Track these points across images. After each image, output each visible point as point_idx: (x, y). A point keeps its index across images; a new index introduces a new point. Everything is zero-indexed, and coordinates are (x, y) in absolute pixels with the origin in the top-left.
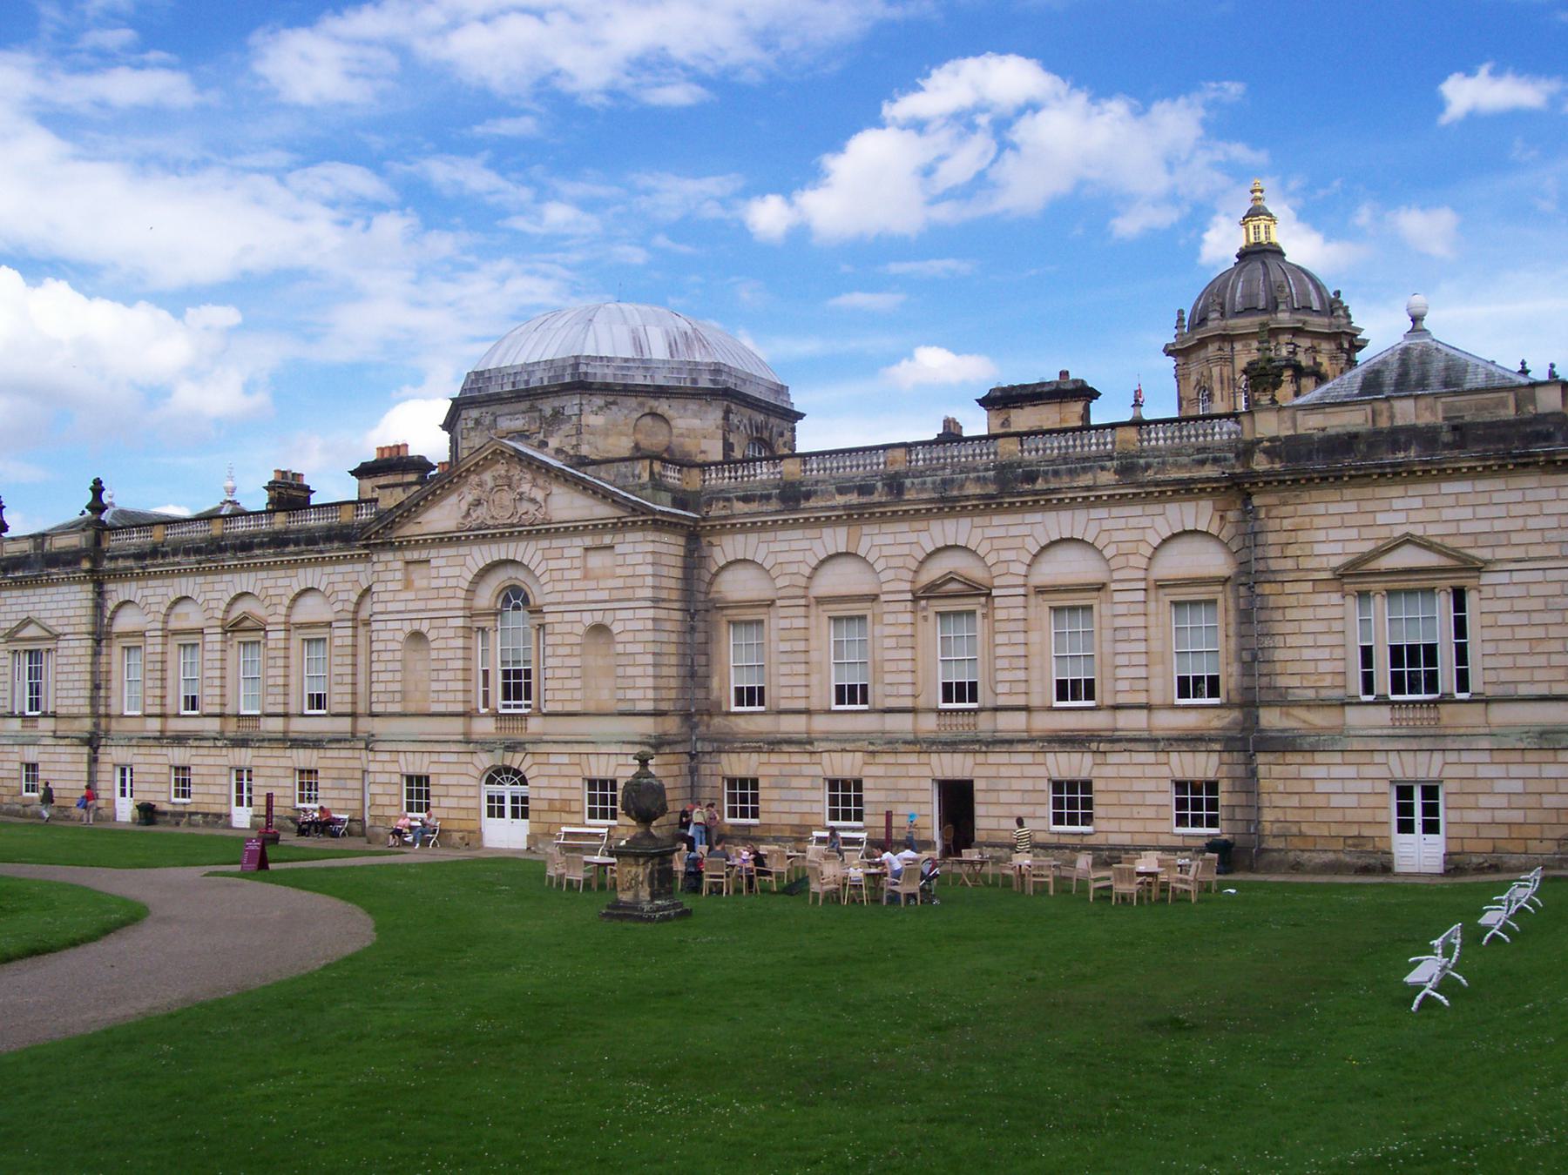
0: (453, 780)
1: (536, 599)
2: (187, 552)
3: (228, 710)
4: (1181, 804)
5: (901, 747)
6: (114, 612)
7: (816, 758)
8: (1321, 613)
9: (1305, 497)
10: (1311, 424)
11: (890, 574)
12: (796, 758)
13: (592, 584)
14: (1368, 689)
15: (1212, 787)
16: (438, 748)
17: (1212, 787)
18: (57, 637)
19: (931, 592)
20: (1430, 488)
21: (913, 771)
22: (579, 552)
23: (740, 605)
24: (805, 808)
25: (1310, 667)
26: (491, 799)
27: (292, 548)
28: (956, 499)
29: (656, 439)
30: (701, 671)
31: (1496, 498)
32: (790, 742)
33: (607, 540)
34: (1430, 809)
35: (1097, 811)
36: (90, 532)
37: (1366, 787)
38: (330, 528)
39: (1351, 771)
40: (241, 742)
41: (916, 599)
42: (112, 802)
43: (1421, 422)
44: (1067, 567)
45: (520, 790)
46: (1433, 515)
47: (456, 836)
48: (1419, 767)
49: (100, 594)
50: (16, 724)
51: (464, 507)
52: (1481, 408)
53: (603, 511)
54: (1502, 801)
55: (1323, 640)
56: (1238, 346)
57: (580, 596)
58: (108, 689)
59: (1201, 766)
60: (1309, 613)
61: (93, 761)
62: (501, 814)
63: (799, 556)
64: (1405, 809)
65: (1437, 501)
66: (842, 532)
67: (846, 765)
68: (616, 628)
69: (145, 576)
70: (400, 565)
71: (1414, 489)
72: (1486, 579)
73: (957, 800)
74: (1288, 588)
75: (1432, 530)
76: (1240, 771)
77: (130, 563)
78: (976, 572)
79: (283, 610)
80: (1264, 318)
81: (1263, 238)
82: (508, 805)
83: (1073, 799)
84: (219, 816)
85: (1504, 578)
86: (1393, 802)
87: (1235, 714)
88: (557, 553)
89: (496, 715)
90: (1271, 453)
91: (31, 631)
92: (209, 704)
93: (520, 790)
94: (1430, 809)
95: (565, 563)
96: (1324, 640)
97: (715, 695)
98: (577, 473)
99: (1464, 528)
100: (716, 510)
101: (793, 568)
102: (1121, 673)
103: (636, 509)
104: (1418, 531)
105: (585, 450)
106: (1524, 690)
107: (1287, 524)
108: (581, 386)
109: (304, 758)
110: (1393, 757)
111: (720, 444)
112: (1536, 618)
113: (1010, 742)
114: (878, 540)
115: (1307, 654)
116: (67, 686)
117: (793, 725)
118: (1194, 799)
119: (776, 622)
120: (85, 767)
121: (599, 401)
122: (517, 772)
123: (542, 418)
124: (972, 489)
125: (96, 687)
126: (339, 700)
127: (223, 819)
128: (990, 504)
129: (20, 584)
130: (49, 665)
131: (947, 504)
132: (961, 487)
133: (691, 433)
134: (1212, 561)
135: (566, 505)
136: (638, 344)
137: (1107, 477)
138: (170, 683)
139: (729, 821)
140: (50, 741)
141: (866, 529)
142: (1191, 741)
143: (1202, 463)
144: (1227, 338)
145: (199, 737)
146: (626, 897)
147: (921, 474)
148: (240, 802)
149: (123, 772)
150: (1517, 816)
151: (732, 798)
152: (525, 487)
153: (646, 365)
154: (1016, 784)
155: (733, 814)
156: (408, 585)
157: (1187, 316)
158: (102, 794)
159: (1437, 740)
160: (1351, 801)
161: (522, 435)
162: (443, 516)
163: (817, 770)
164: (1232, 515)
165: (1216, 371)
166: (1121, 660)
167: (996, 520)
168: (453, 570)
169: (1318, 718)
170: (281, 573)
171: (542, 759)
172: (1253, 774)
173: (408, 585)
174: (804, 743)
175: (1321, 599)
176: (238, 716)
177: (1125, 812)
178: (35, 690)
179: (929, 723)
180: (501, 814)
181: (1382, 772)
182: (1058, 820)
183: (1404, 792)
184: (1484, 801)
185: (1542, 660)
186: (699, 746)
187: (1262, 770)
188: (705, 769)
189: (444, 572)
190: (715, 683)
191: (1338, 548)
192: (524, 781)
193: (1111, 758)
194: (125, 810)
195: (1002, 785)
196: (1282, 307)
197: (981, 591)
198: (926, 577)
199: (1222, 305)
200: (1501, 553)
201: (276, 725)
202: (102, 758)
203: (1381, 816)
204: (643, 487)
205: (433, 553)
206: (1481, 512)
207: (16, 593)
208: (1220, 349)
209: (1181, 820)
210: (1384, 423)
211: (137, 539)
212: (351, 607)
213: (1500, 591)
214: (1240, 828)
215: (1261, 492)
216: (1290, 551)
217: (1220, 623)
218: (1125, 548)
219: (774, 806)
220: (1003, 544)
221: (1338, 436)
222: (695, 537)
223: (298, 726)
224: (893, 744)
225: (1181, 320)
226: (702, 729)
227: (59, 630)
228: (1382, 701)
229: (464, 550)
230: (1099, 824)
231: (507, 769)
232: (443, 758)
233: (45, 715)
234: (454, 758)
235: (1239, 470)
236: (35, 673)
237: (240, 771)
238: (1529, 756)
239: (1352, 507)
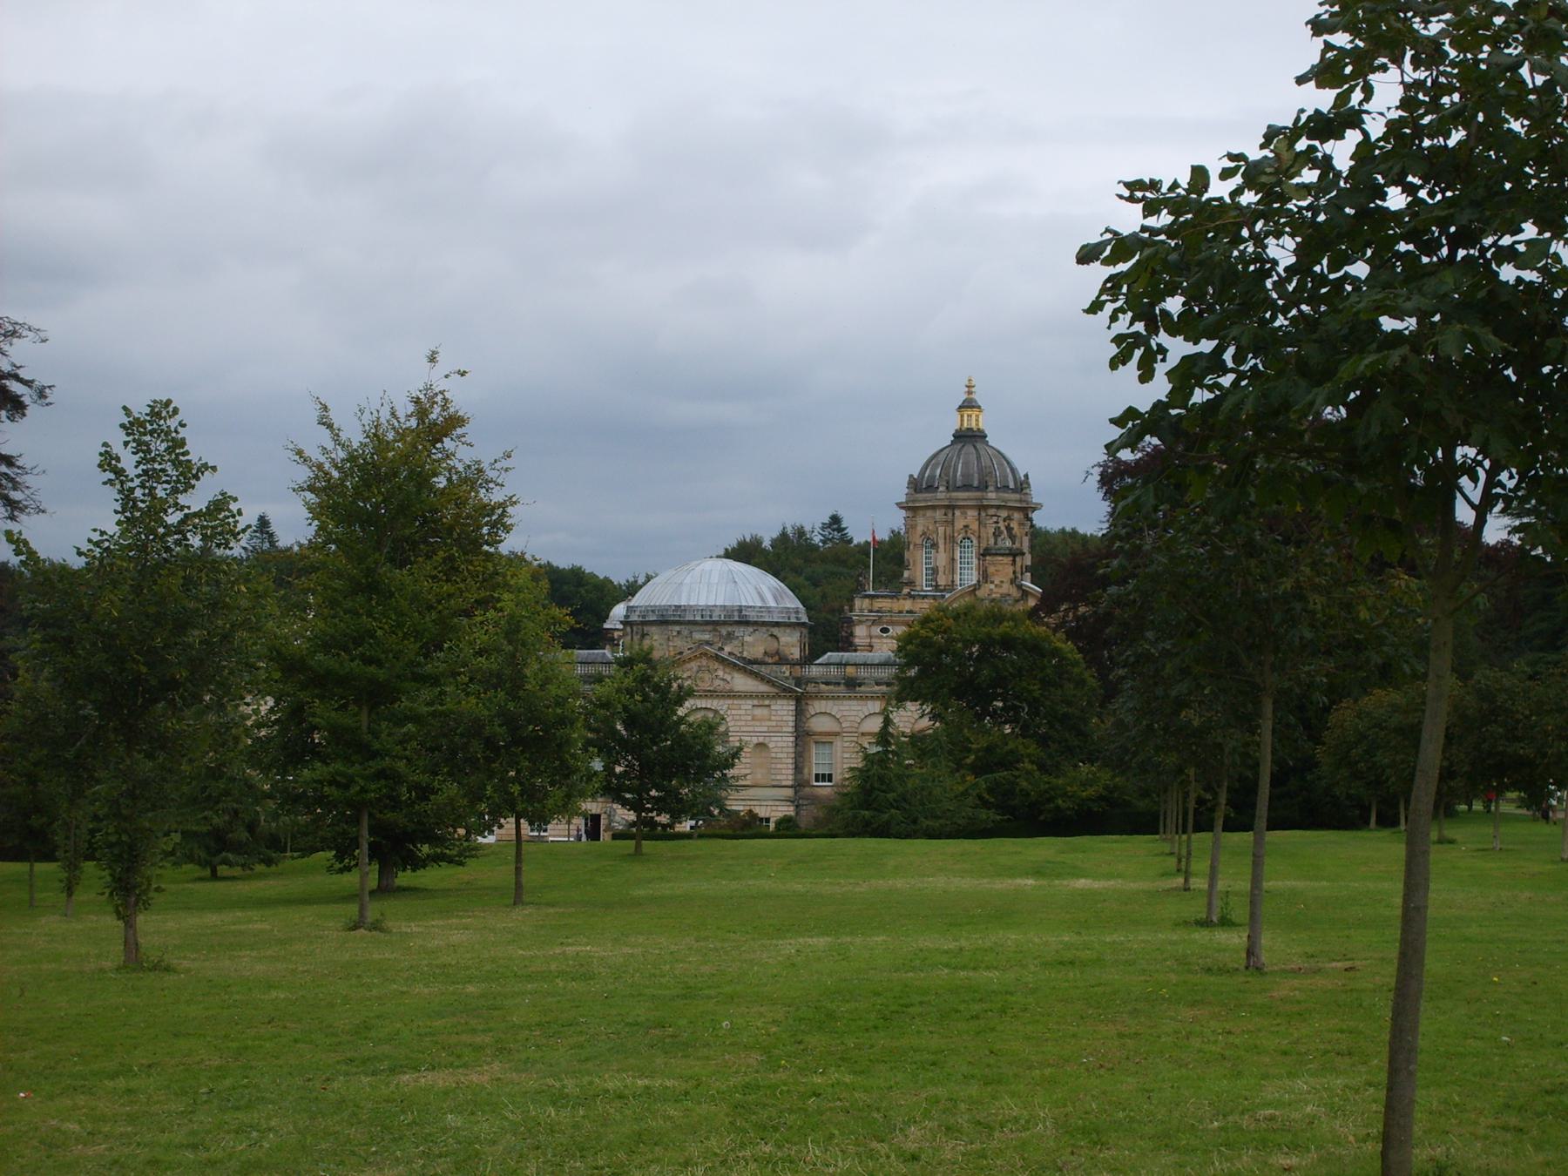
23: (820, 734)
53: (763, 688)
80: (978, 494)
81: (974, 425)
98: (747, 666)
100: (810, 688)
108: (745, 623)
119: (838, 743)
123: (721, 636)
133: (787, 645)
135: (741, 682)
152: (720, 673)
153: (769, 610)
165: (941, 530)
222: (800, 701)
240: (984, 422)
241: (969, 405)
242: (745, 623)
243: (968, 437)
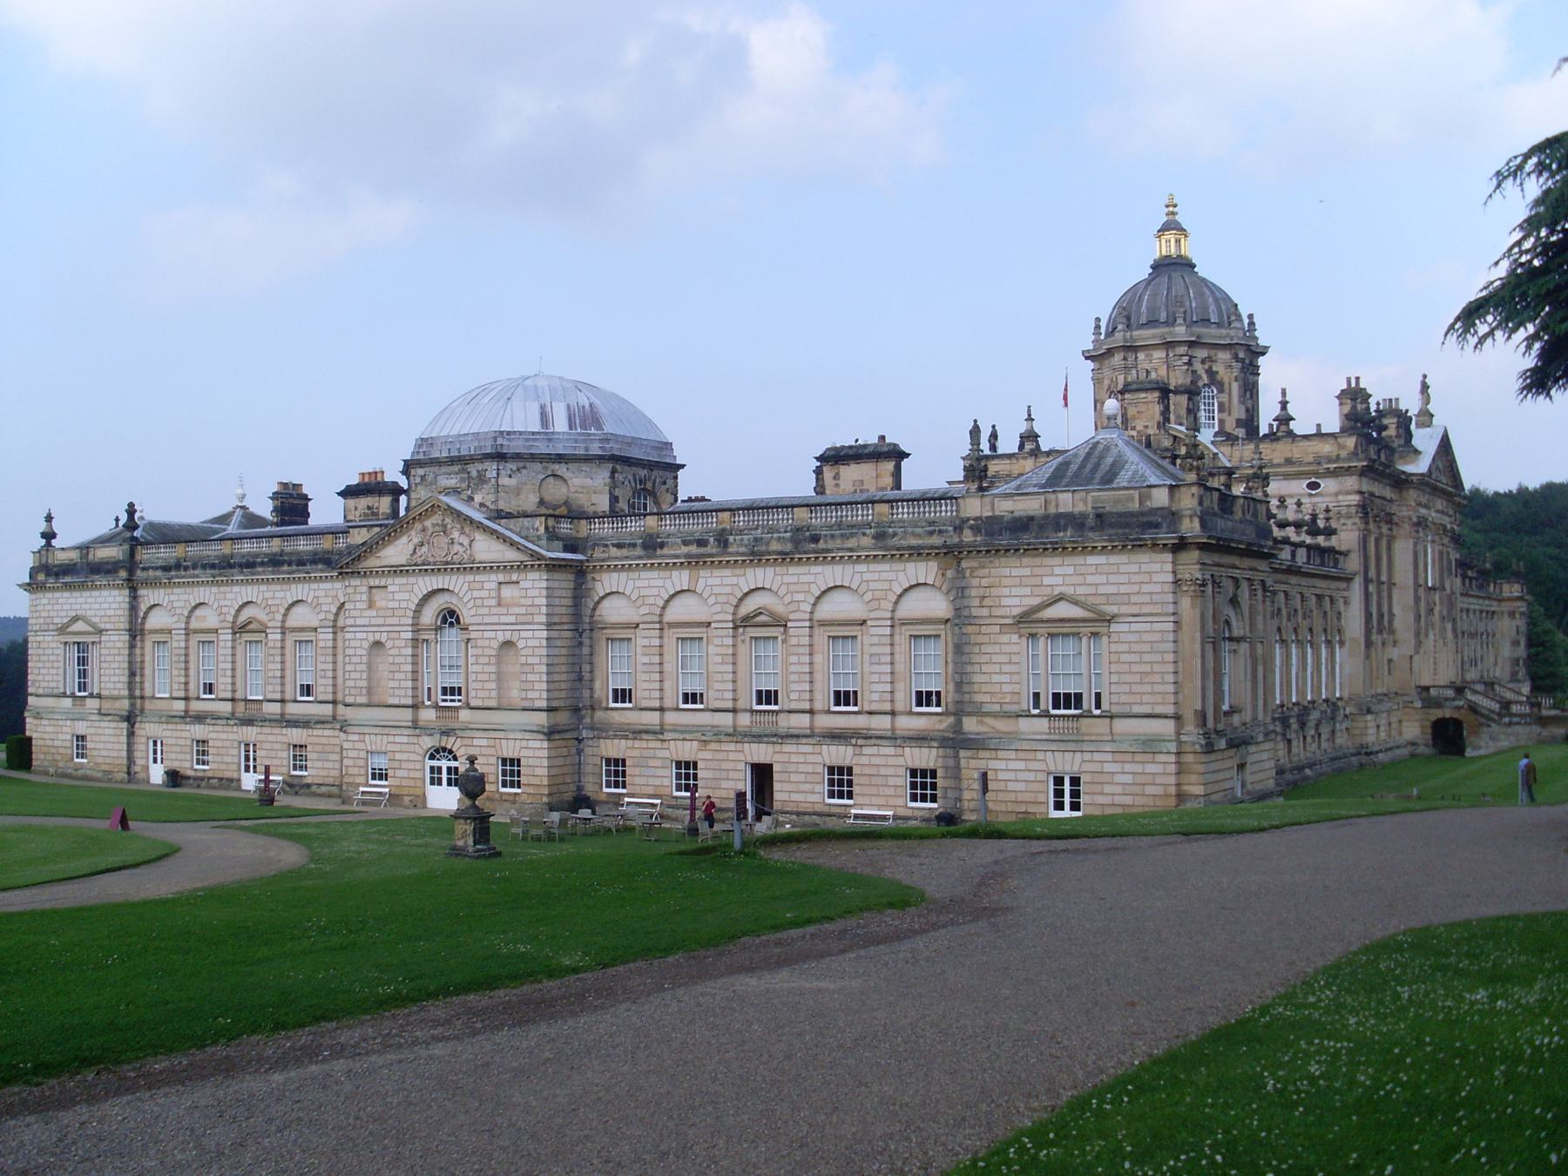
0: (404, 756)
1: (466, 618)
2: (204, 567)
3: (239, 695)
4: (914, 786)
5: (724, 738)
6: (146, 613)
7: (665, 745)
8: (1006, 649)
9: (997, 562)
10: (1005, 507)
11: (717, 608)
12: (652, 744)
13: (504, 610)
14: (1036, 706)
15: (934, 773)
16: (393, 731)
17: (934, 773)
18: (101, 632)
19: (743, 623)
20: (1079, 560)
21: (732, 756)
22: (494, 585)
23: (615, 626)
24: (658, 782)
25: (997, 688)
26: (432, 768)
27: (285, 568)
28: (762, 554)
29: (555, 492)
30: (587, 676)
31: (1123, 569)
32: (647, 732)
33: (514, 577)
34: (1075, 794)
35: (856, 789)
36: (126, 547)
37: (1031, 776)
38: (315, 553)
39: (1021, 765)
40: (249, 722)
41: (735, 628)
42: (147, 768)
43: (1077, 510)
44: (839, 606)
45: (453, 764)
46: (1080, 580)
47: (407, 799)
48: (1068, 764)
49: (134, 598)
50: (68, 702)
51: (411, 547)
52: (1117, 501)
53: (512, 555)
54: (1119, 789)
55: (1006, 668)
56: (1141, 356)
57: (495, 619)
58: (142, 675)
59: (926, 757)
60: (997, 649)
61: (131, 734)
62: (440, 783)
63: (655, 592)
64: (1059, 793)
65: (1083, 570)
66: (685, 574)
67: (687, 751)
68: (521, 644)
69: (170, 584)
70: (365, 589)
71: (1068, 560)
72: (1114, 628)
73: (762, 775)
74: (984, 629)
75: (1081, 590)
76: (951, 762)
77: (159, 573)
78: (780, 609)
79: (280, 617)
82: (444, 776)
83: (841, 780)
84: (231, 780)
85: (1125, 627)
86: (1052, 787)
87: (951, 719)
88: (478, 586)
89: (436, 706)
90: (976, 530)
91: (79, 626)
92: (223, 690)
93: (453, 764)
94: (1075, 794)
95: (485, 594)
96: (1010, 670)
97: (597, 694)
99: (1102, 590)
101: (652, 600)
102: (875, 687)
103: (535, 556)
104: (1069, 591)
105: (502, 505)
106: (1136, 709)
107: (984, 582)
108: (500, 457)
109: (296, 735)
110: (1049, 754)
111: (607, 497)
112: (1146, 658)
113: (798, 736)
114: (711, 581)
115: (996, 678)
116: (109, 675)
117: (652, 719)
118: (923, 784)
120: (124, 739)
121: (512, 466)
122: (451, 752)
124: (775, 546)
125: (132, 674)
126: (323, 690)
127: (234, 783)
128: (785, 558)
129: (68, 587)
130: (94, 654)
131: (756, 556)
132: (768, 544)
134: (936, 604)
135: (486, 549)
136: (544, 418)
137: (867, 541)
138: (192, 672)
139: (605, 790)
140: (96, 717)
141: (702, 573)
142: (920, 739)
143: (931, 533)
144: (1130, 349)
145: (215, 717)
146: (460, 843)
147: (741, 532)
148: (247, 769)
149: (155, 743)
150: (1128, 800)
151: (608, 773)
152: (456, 534)
153: (549, 437)
154: (802, 768)
155: (608, 786)
156: (371, 605)
157: (1103, 325)
158: (139, 762)
159: (1076, 743)
160: (1021, 786)
161: (456, 491)
162: (397, 552)
163: (666, 754)
164: (950, 573)
166: (875, 678)
167: (792, 570)
168: (404, 593)
169: (1002, 725)
170: (278, 587)
171: (468, 742)
172: (958, 768)
173: (371, 605)
174: (658, 732)
175: (1005, 638)
176: (246, 700)
177: (874, 791)
178: (83, 674)
179: (744, 720)
180: (440, 783)
181: (1042, 766)
182: (831, 795)
183: (1059, 781)
184: (1107, 789)
185: (1147, 688)
186: (584, 733)
187: (963, 762)
188: (588, 751)
189: (398, 596)
190: (597, 685)
191: (1016, 601)
192: (455, 759)
193: (866, 750)
194: (157, 775)
195: (792, 768)
196: (1180, 321)
197: (781, 623)
198: (745, 610)
199: (1128, 318)
200: (1124, 609)
201: (275, 708)
202: (138, 732)
203: (1041, 798)
204: (539, 538)
205: (390, 581)
206: (1112, 578)
207: (66, 594)
208: (1125, 359)
209: (914, 798)
210: (1052, 510)
211: (164, 554)
212: (332, 617)
213: (1123, 637)
214: (950, 804)
215: (967, 557)
216: (987, 602)
217: (941, 652)
218: (879, 594)
219: (637, 780)
220: (789, 587)
221: (1020, 518)
223: (293, 709)
224: (719, 735)
225: (1098, 327)
226: (587, 720)
227: (102, 626)
228: (1046, 714)
229: (412, 580)
230: (857, 799)
231: (444, 749)
232: (398, 739)
233: (91, 696)
234: (405, 739)
235: (956, 540)
236: (82, 661)
237: (247, 745)
238: (1138, 757)
239: (1027, 571)
240: (1189, 249)
241: (1171, 226)
242: (500, 457)
243: (1173, 267)
